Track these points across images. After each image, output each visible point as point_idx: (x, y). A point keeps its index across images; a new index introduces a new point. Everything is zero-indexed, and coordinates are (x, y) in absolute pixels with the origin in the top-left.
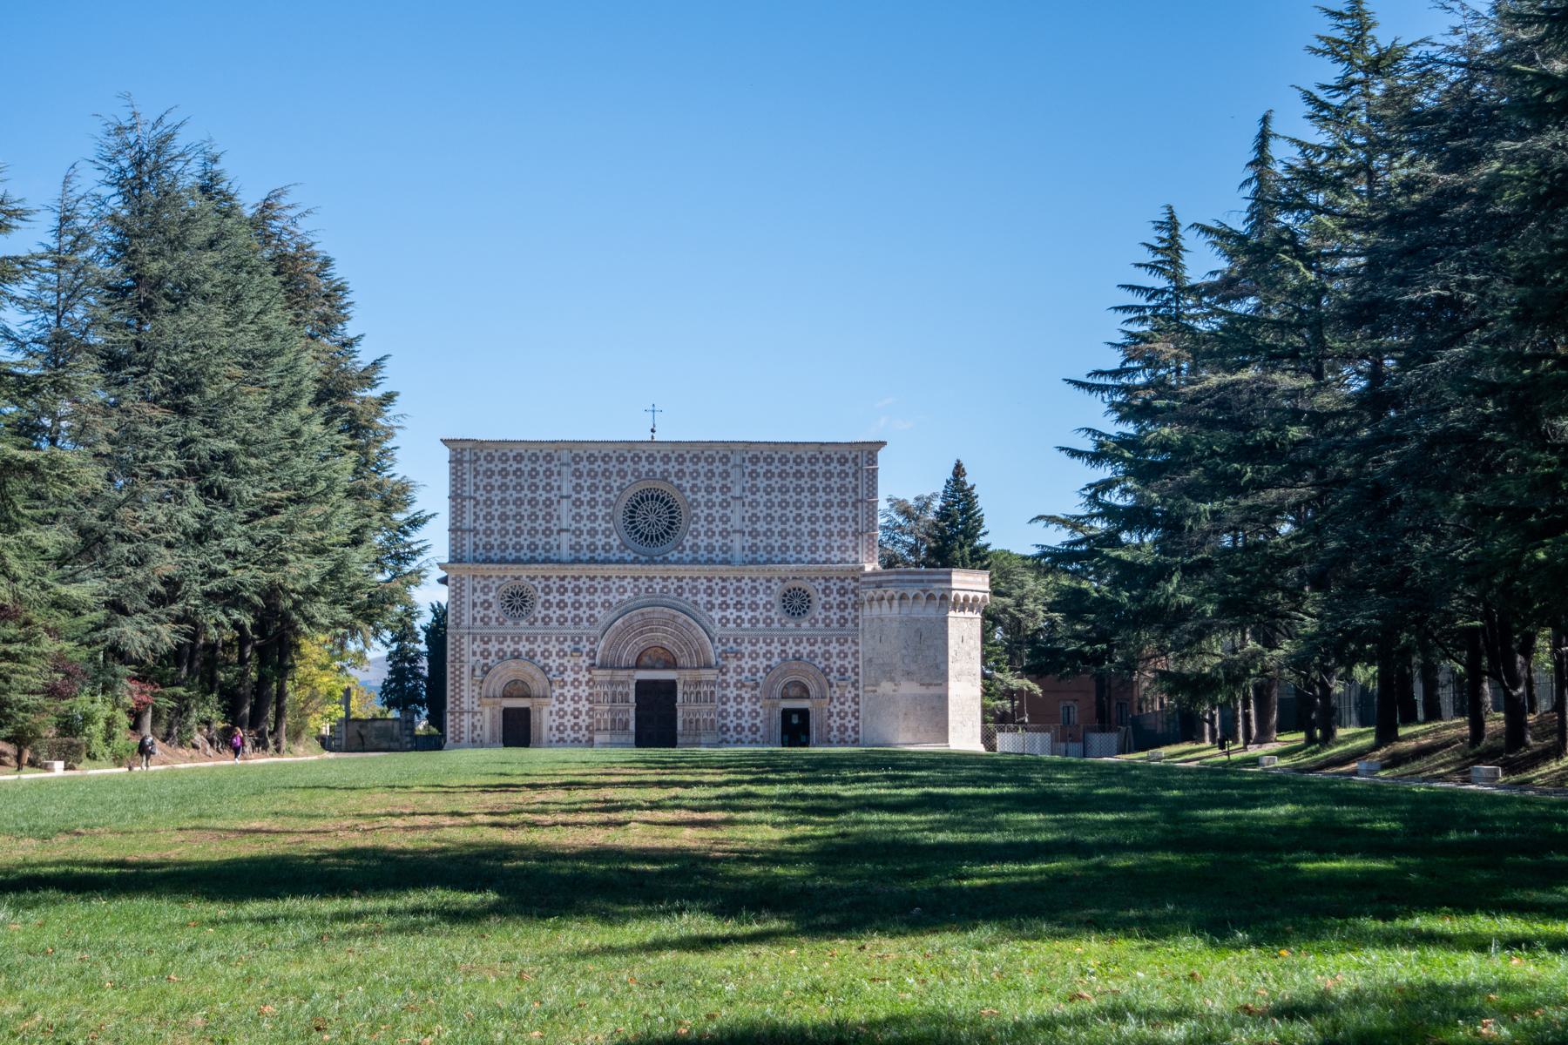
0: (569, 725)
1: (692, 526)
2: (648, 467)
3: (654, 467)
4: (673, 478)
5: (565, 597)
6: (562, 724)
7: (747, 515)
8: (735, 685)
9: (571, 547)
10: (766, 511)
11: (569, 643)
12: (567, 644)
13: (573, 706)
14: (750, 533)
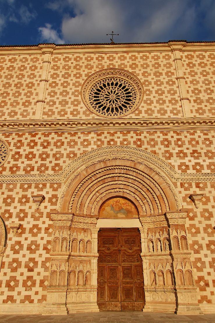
0: (21, 279)
1: (145, 98)
2: (108, 62)
3: (114, 62)
4: (128, 69)
5: (34, 150)
6: (13, 278)
7: (190, 90)
8: (205, 229)
9: (44, 113)
10: (205, 87)
11: (33, 189)
12: (30, 190)
13: (29, 255)
14: (195, 101)
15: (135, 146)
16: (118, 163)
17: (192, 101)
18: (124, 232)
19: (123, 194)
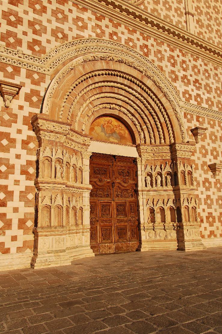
8: (202, 166)
15: (142, 53)
16: (123, 68)
17: (195, 21)
18: (119, 161)
19: (119, 114)
